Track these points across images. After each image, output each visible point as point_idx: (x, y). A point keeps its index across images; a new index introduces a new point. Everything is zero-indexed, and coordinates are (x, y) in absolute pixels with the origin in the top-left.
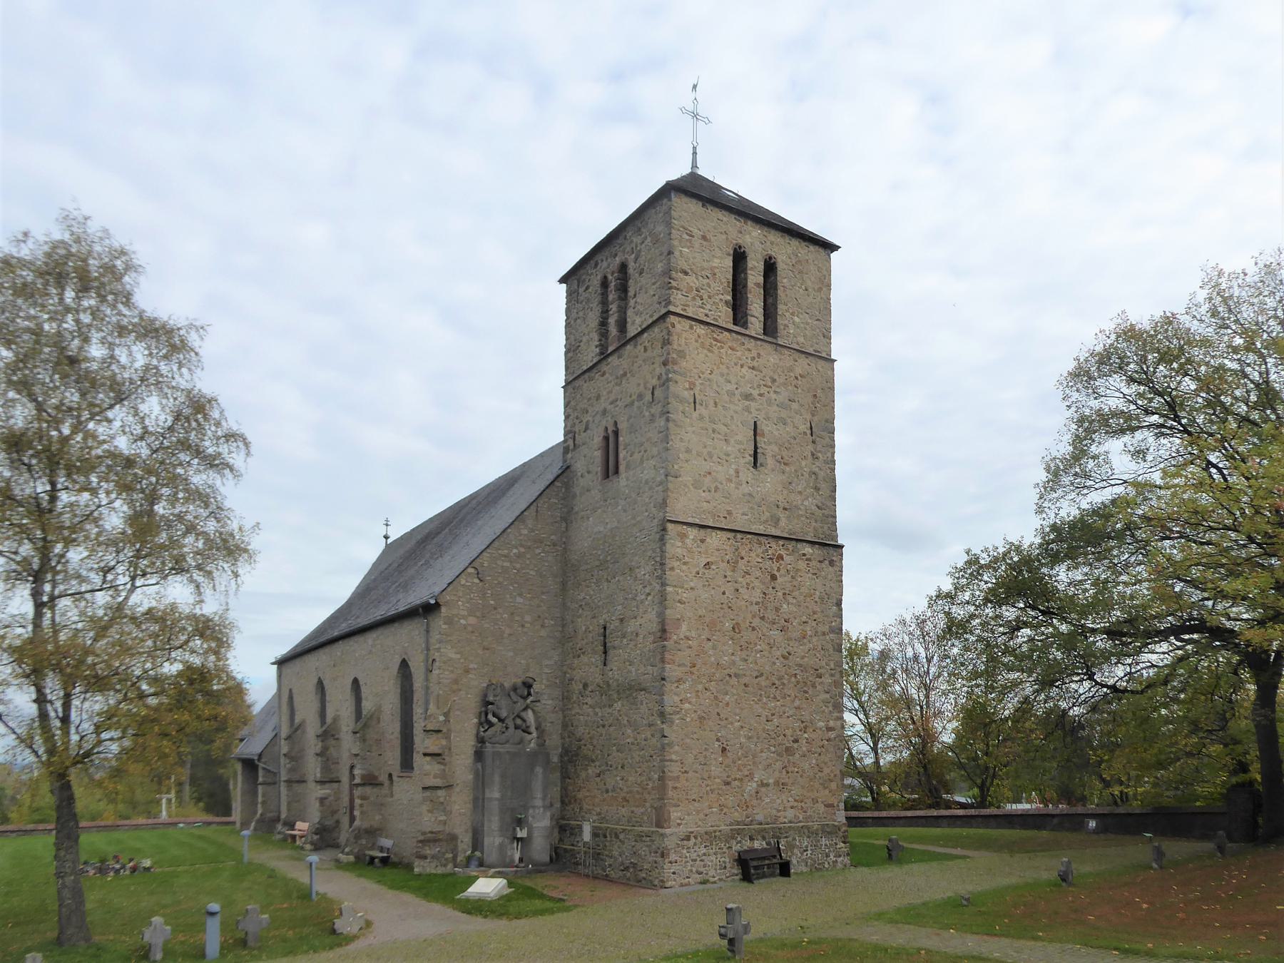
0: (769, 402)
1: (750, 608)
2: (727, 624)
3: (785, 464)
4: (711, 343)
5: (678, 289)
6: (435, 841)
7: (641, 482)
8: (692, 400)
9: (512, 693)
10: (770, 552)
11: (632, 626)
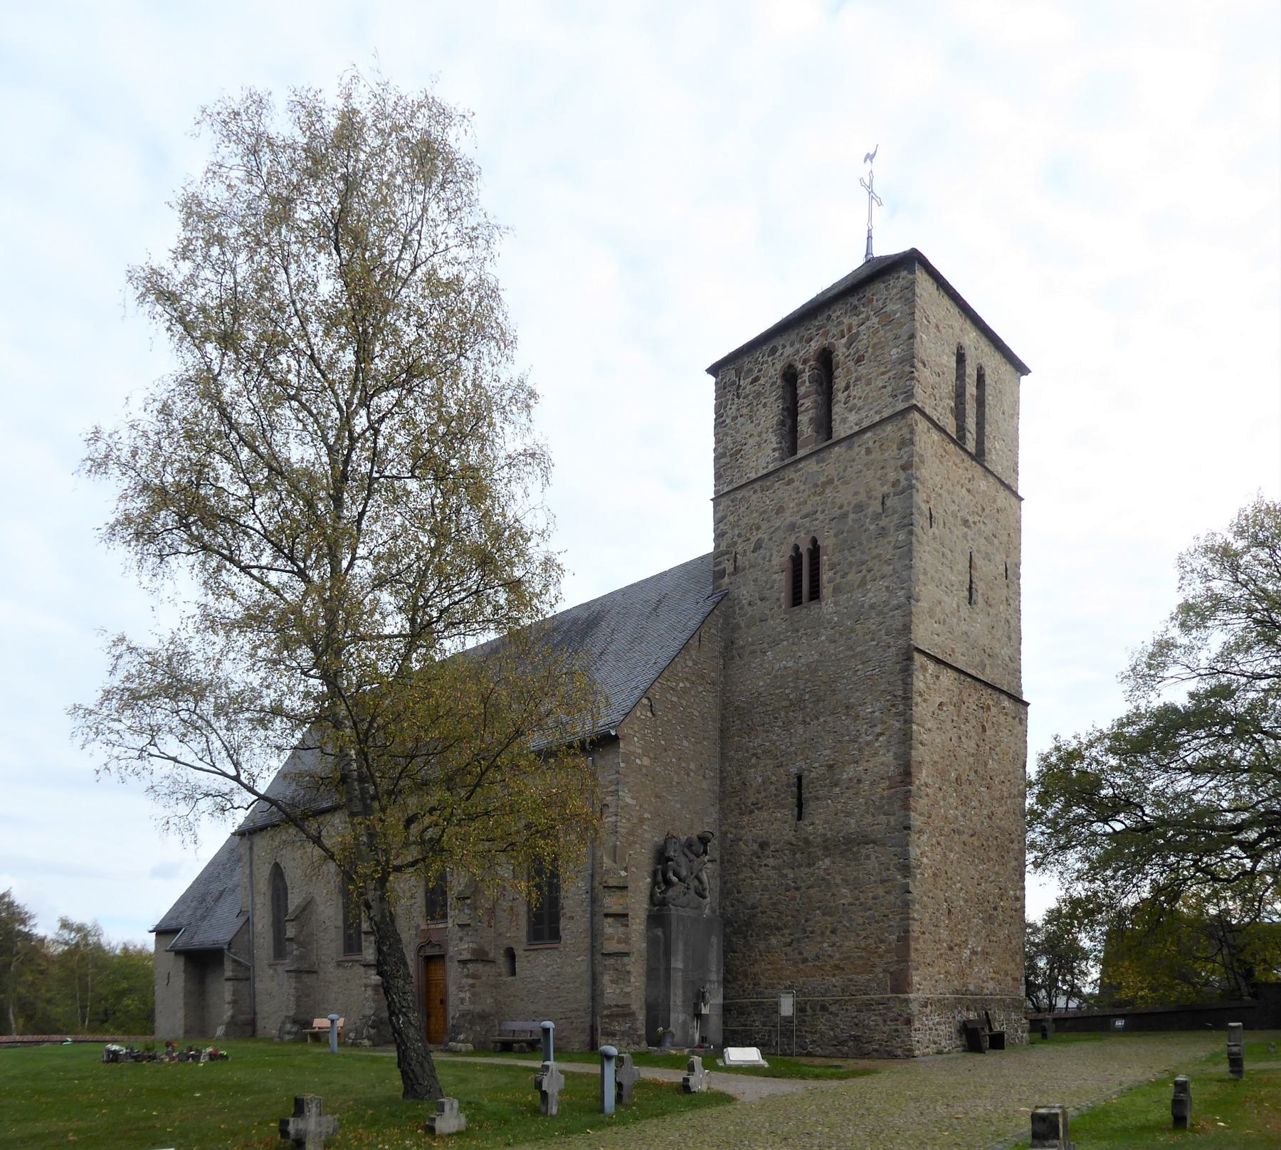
6: (625, 1015)
7: (863, 606)
8: (928, 516)
9: (686, 851)
11: (850, 772)
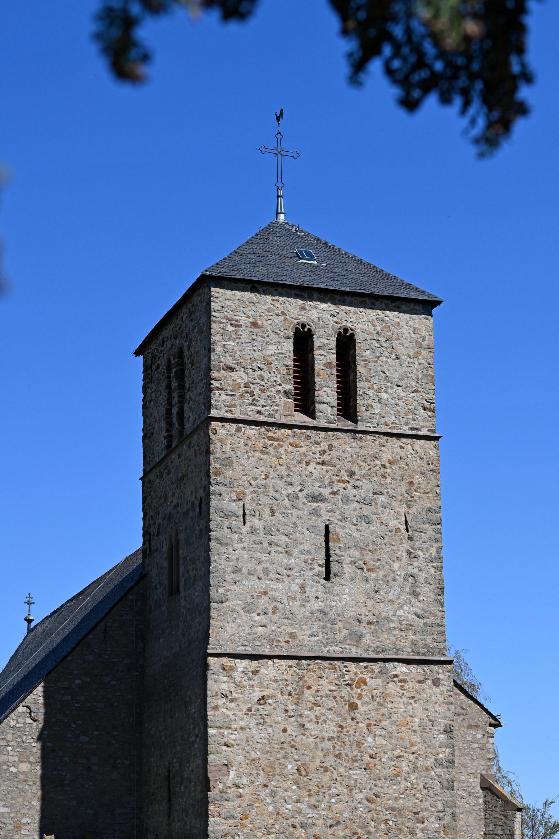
0: (346, 500)
1: (321, 745)
2: (290, 767)
3: (369, 570)
4: (265, 444)
5: (221, 389)
10: (347, 677)
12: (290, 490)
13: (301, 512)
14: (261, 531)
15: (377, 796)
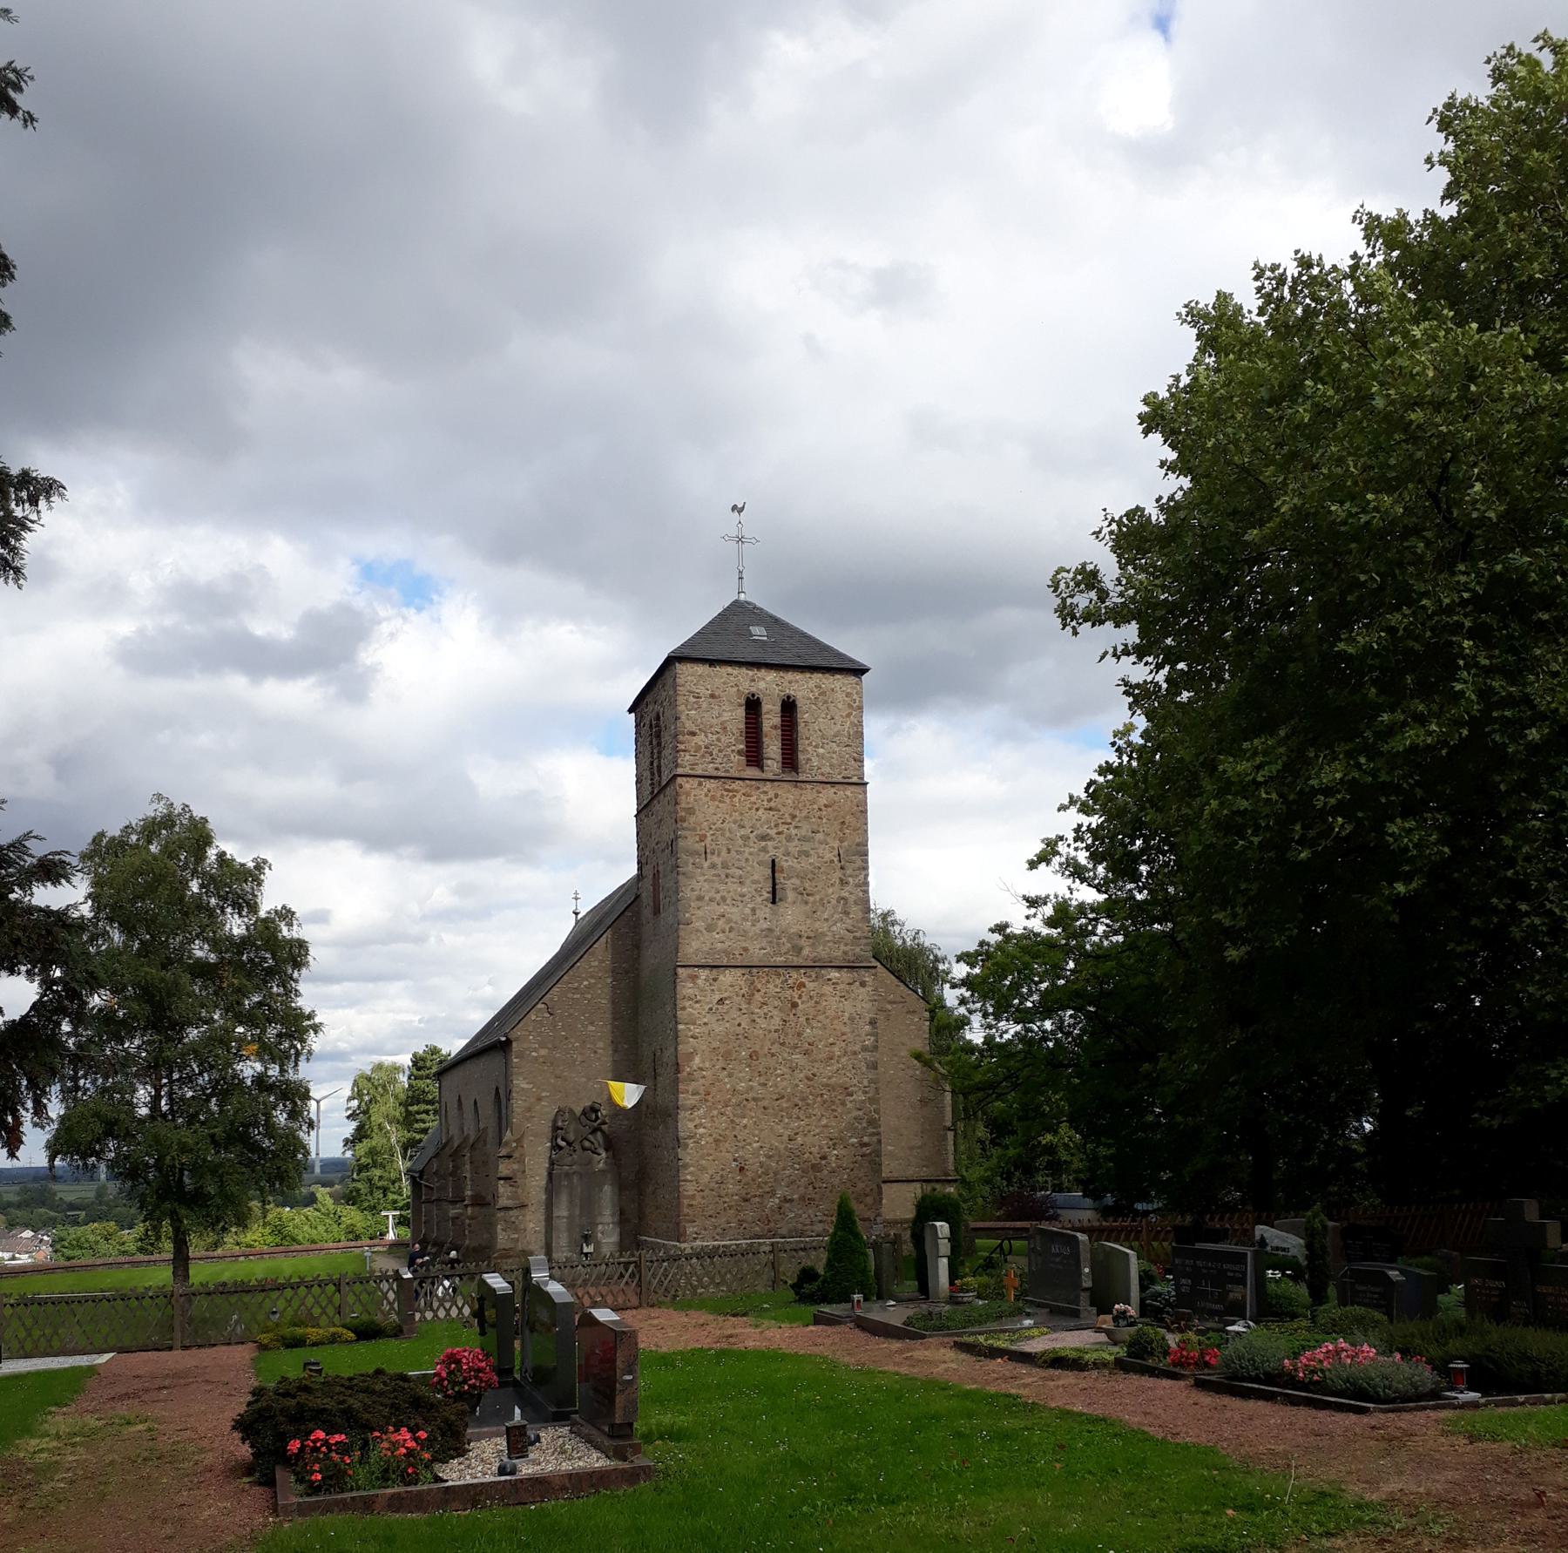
0: (789, 838)
3: (808, 895)
12: (743, 832)
13: (752, 850)
14: (720, 866)
15: (814, 1075)
